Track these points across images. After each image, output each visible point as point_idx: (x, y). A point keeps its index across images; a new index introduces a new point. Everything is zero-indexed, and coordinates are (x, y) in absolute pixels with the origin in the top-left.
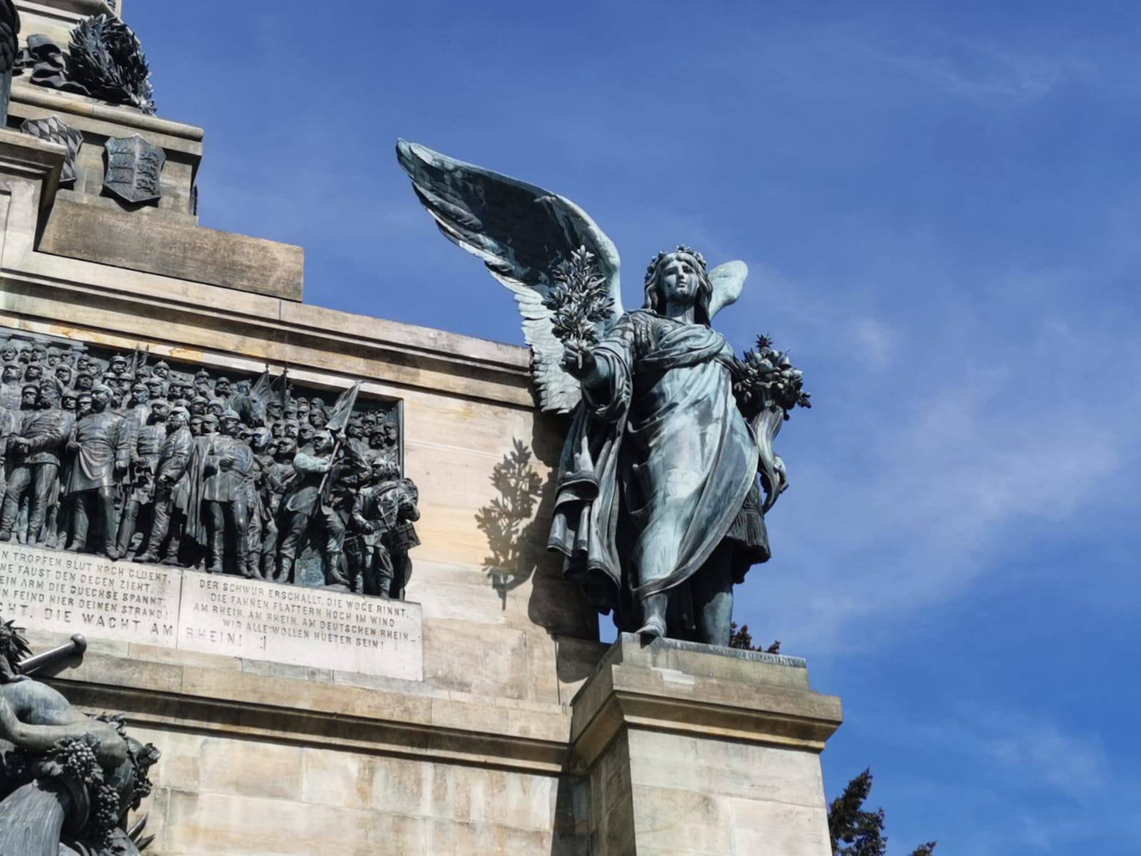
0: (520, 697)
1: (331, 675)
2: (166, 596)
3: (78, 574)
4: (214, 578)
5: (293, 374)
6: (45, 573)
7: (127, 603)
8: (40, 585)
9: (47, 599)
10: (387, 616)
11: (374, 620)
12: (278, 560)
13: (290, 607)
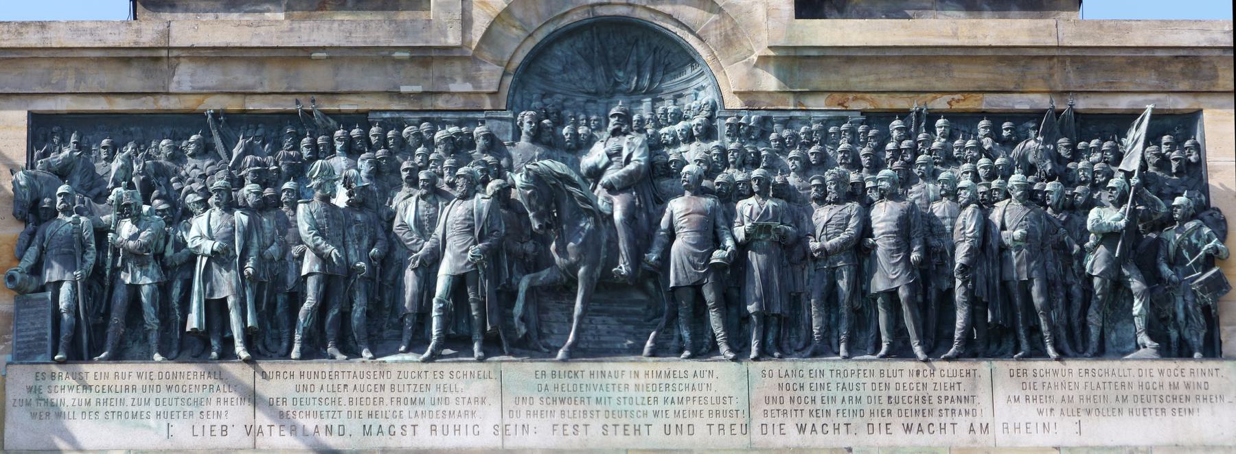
2: (979, 393)
3: (893, 381)
4: (1025, 365)
5: (1082, 104)
6: (861, 386)
7: (943, 406)
8: (859, 400)
10: (1201, 379)
11: (1188, 386)
12: (1085, 326)
13: (1101, 385)
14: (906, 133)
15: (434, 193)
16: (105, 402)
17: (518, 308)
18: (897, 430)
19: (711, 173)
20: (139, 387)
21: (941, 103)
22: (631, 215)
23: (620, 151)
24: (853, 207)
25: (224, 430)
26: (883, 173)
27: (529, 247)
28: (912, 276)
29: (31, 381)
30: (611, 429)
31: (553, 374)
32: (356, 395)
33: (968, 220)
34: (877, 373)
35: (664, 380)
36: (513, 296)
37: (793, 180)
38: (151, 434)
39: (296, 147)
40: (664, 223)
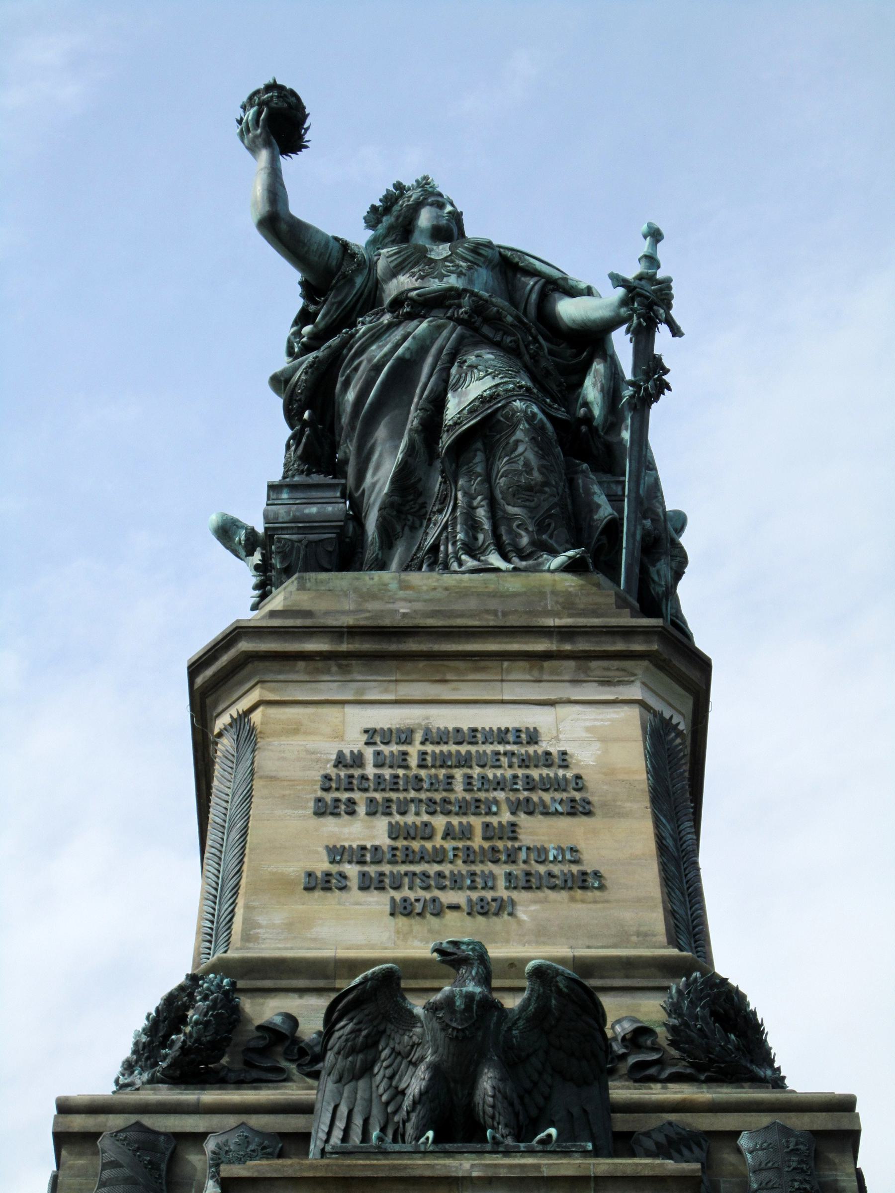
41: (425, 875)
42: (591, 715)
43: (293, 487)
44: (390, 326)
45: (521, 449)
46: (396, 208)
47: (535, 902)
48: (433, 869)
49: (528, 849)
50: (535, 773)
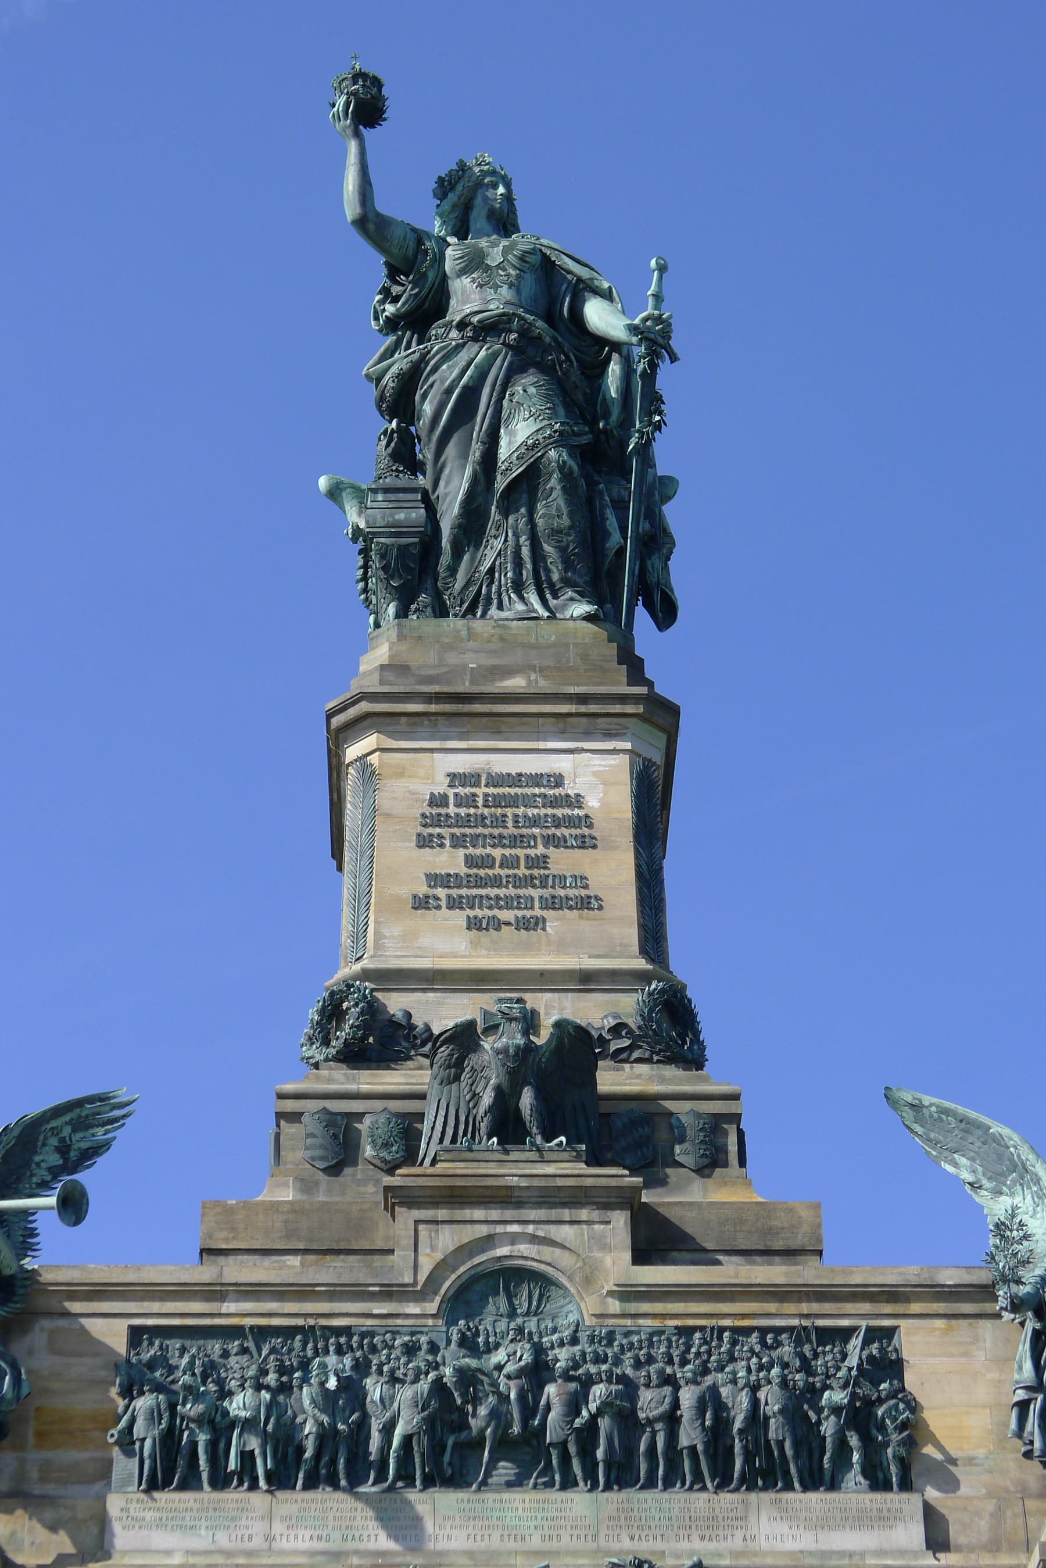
0: (998, 1550)
1: (862, 1555)
5: (821, 1323)
9: (675, 1528)
10: (898, 1506)
11: (889, 1510)
14: (705, 1342)
15: (394, 1380)
16: (172, 1518)
17: (447, 1458)
18: (695, 1539)
19: (576, 1366)
20: (195, 1508)
21: (727, 1322)
22: (522, 1396)
23: (515, 1353)
24: (667, 1390)
25: (250, 1537)
26: (690, 1367)
27: (455, 1416)
28: (707, 1435)
29: (123, 1505)
30: (506, 1538)
31: (469, 1501)
32: (338, 1514)
33: (744, 1399)
34: (682, 1501)
35: (541, 1505)
36: (443, 1449)
37: (629, 1371)
38: (201, 1540)
39: (304, 1349)
40: (543, 1402)
41: (489, 898)
42: (597, 760)
43: (387, 490)
44: (459, 347)
45: (554, 495)
46: (459, 188)
47: (557, 919)
48: (493, 892)
49: (554, 876)
50: (559, 812)
